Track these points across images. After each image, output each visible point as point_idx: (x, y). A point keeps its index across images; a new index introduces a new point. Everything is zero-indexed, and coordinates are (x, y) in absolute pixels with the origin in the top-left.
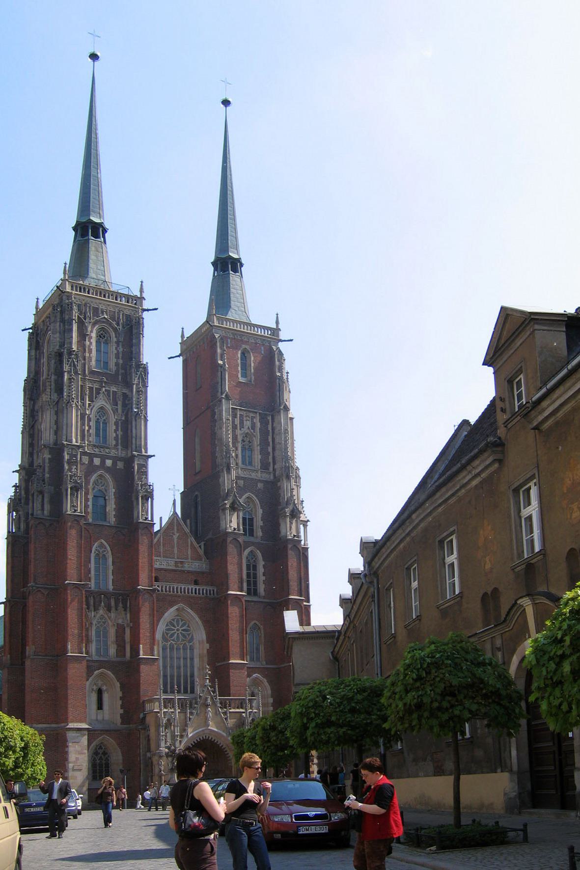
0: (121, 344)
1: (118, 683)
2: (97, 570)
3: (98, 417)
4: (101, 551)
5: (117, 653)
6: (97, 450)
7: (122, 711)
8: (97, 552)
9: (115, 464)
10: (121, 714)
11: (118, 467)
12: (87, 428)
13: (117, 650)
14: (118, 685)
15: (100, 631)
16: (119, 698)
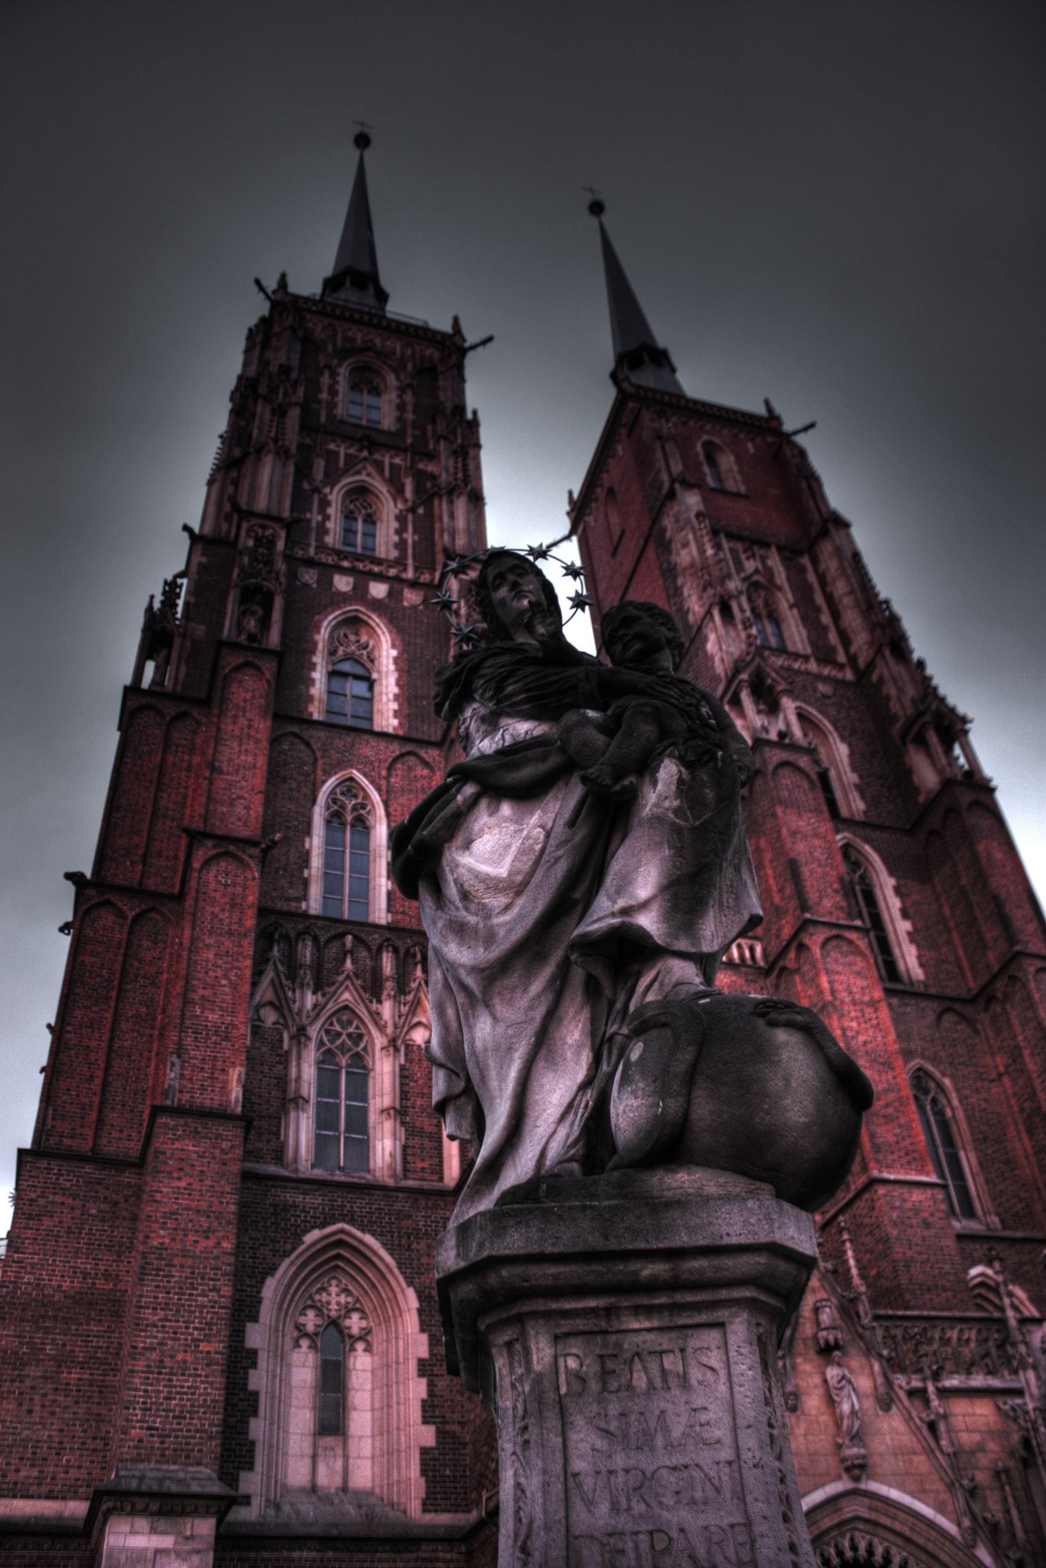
0: (409, 392)
1: (411, 1294)
2: (332, 859)
3: (352, 507)
4: (350, 804)
5: (405, 1161)
6: (345, 564)
7: (428, 1435)
8: (336, 807)
9: (394, 594)
10: (424, 1451)
11: (405, 604)
12: (320, 518)
13: (405, 1148)
14: (411, 1300)
15: (338, 1072)
16: (413, 1366)
